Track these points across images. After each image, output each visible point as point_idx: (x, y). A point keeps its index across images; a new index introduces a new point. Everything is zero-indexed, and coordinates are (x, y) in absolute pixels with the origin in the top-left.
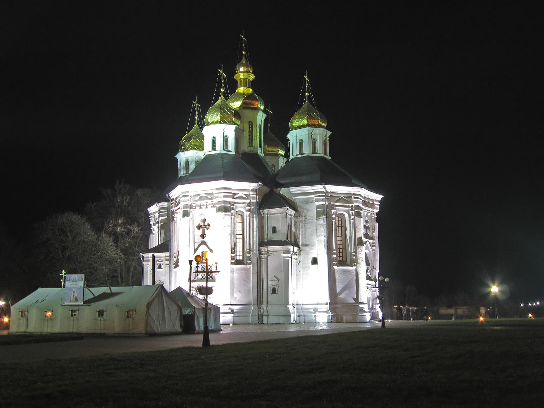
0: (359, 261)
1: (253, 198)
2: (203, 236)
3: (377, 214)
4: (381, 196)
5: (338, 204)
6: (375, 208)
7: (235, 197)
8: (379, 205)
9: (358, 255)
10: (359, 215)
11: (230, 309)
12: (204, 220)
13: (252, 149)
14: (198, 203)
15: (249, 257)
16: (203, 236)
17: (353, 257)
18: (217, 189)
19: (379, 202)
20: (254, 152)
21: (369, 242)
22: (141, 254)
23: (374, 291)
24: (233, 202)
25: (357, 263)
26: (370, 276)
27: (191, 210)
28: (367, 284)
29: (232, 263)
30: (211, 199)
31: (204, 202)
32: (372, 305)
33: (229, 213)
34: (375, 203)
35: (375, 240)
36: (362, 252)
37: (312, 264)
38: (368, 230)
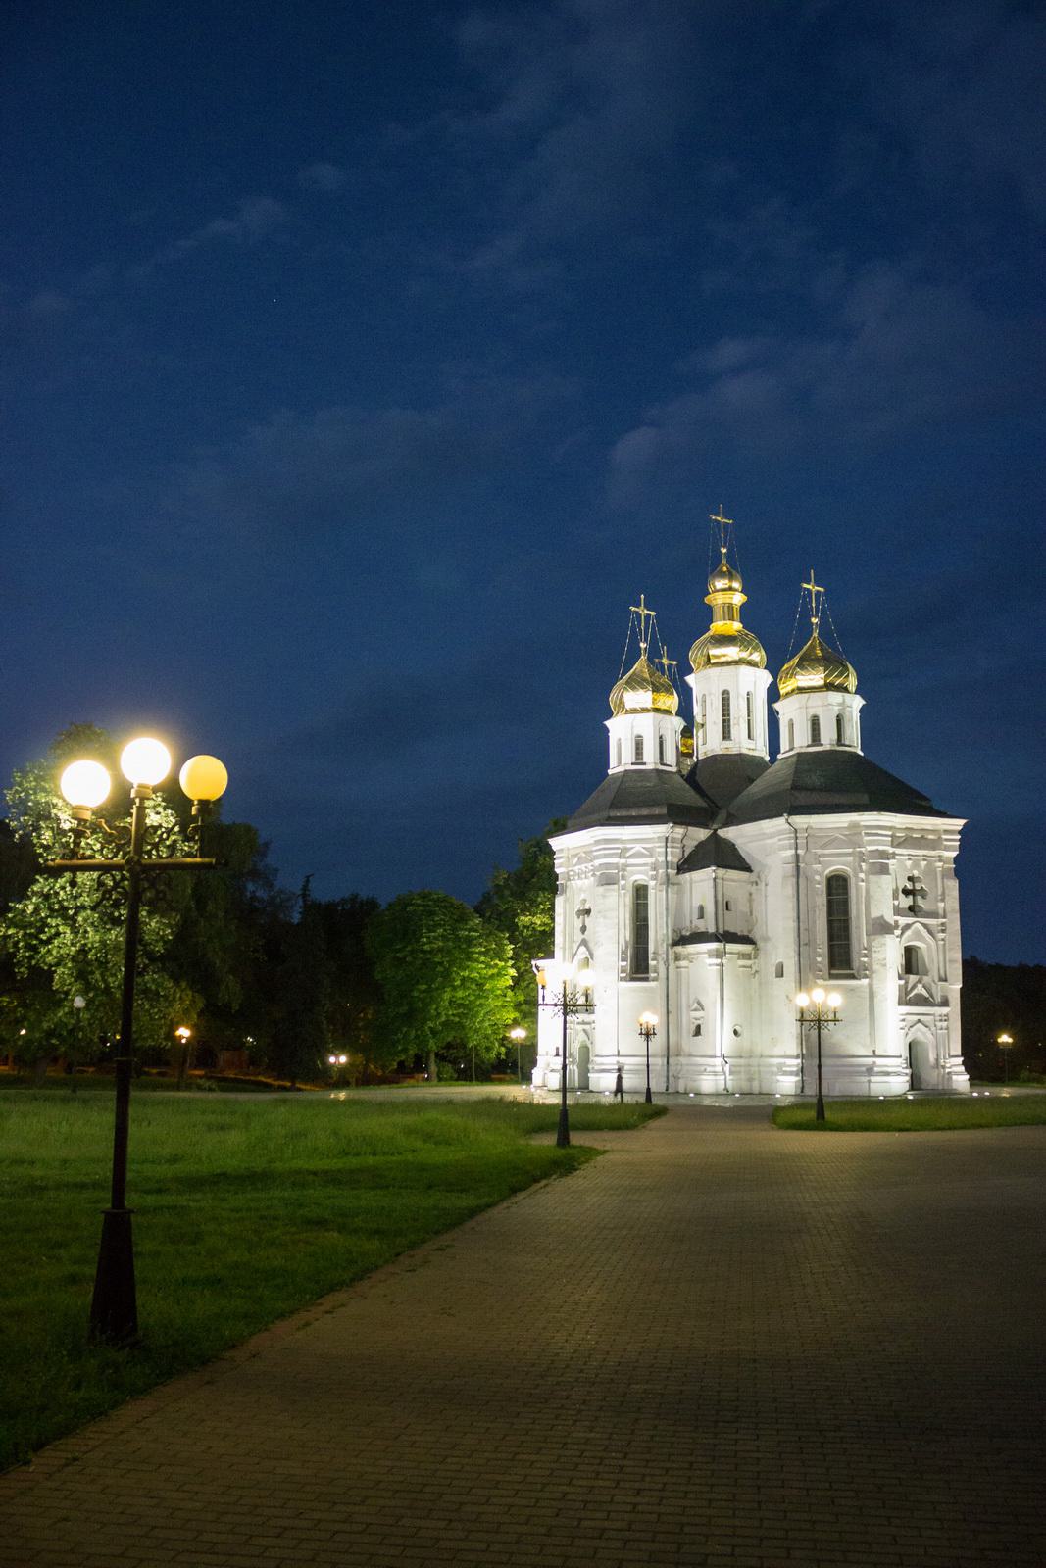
0: (876, 967)
1: (659, 854)
2: (584, 929)
3: (956, 860)
4: (962, 822)
5: (827, 851)
6: (947, 848)
7: (628, 854)
8: (960, 840)
9: (874, 955)
10: (884, 870)
11: (618, 1062)
12: (585, 900)
13: (728, 744)
14: (576, 869)
15: (655, 966)
16: (584, 929)
17: (862, 959)
18: (597, 842)
19: (960, 832)
20: (735, 751)
21: (922, 924)
22: (533, 963)
23: (941, 1029)
24: (623, 865)
25: (873, 972)
26: (927, 995)
27: (568, 883)
28: (902, 1015)
29: (621, 979)
30: (591, 861)
31: (583, 867)
32: (937, 1060)
33: (616, 886)
34: (944, 837)
35: (944, 917)
36: (889, 953)
37: (777, 977)
38: (919, 898)
